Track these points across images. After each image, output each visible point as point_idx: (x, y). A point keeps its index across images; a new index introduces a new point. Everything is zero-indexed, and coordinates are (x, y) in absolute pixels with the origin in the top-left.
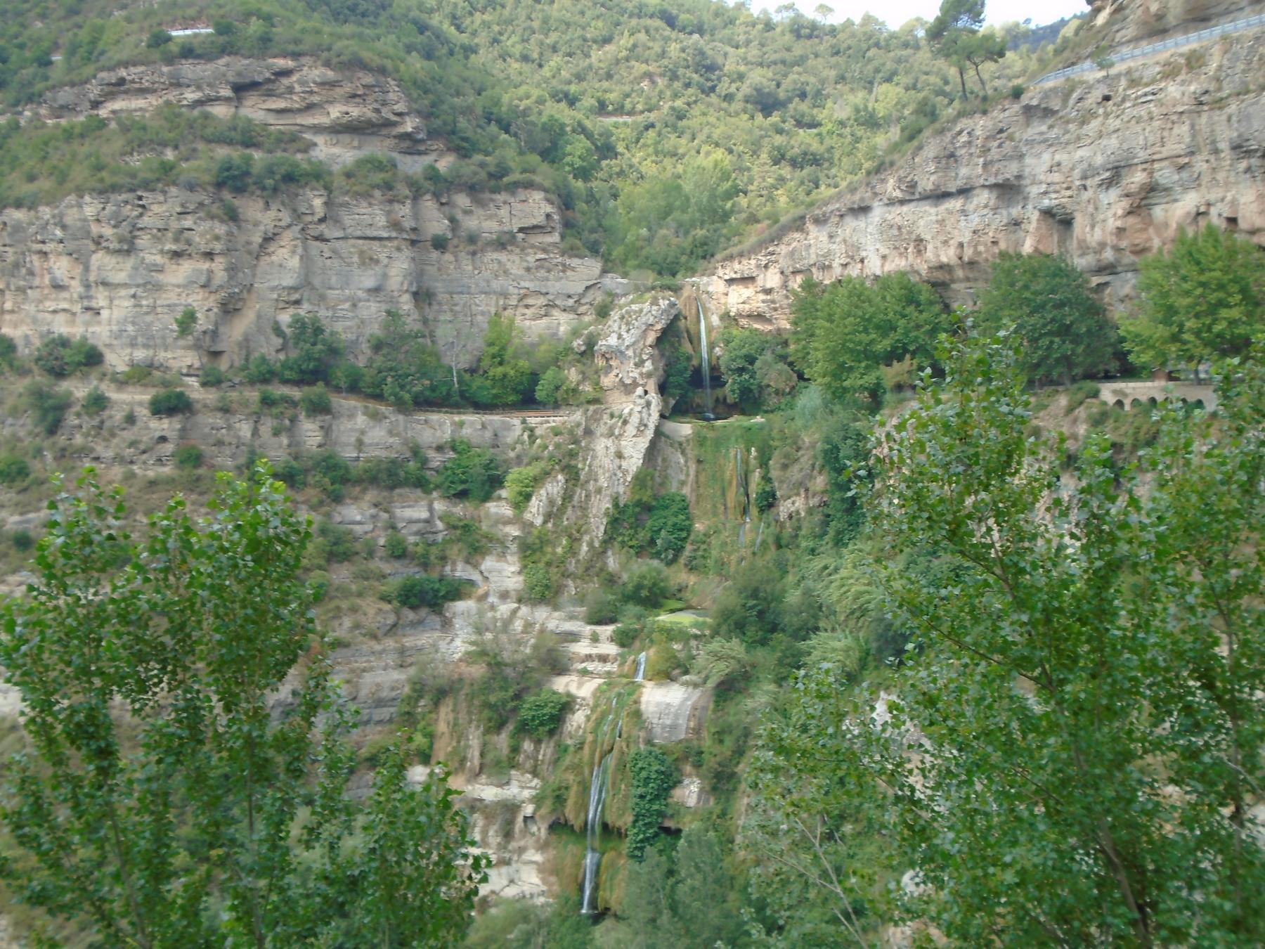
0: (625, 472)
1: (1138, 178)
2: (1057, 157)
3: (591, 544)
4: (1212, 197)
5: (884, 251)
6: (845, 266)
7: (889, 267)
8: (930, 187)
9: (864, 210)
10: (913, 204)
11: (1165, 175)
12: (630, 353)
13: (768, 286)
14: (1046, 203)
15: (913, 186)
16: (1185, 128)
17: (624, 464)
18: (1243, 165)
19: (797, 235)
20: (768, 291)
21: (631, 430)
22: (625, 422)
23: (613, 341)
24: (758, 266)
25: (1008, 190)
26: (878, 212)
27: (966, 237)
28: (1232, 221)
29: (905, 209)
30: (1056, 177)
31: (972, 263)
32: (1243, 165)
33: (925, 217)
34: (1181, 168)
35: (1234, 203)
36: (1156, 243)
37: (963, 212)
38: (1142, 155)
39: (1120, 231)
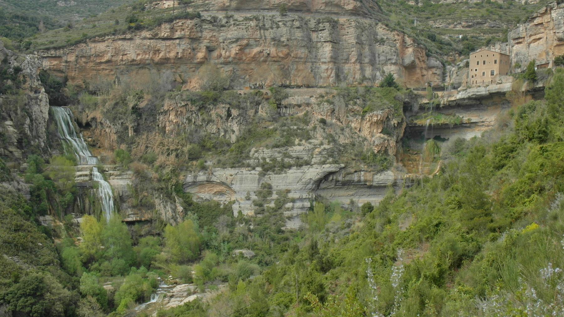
0: (44, 118)
1: (245, 42)
2: (214, 34)
3: (43, 142)
4: (264, 48)
5: (138, 52)
6: (112, 56)
7: (139, 57)
8: (166, 35)
9: (131, 39)
10: (154, 40)
11: (252, 42)
12: (34, 76)
13: (69, 60)
14: (208, 45)
15: (157, 34)
16: (258, 32)
17: (44, 116)
18: (273, 43)
19: (84, 45)
20: (66, 62)
21: (43, 103)
22: (41, 101)
23: (29, 71)
24: (63, 53)
25: (194, 40)
26: (138, 41)
27: (181, 51)
28: (269, 54)
29: (152, 41)
30: (213, 39)
31: (181, 58)
32: (273, 43)
33: (161, 45)
34: (256, 41)
35: (270, 51)
36: (244, 58)
37: (179, 44)
38: (247, 37)
39: (237, 54)
